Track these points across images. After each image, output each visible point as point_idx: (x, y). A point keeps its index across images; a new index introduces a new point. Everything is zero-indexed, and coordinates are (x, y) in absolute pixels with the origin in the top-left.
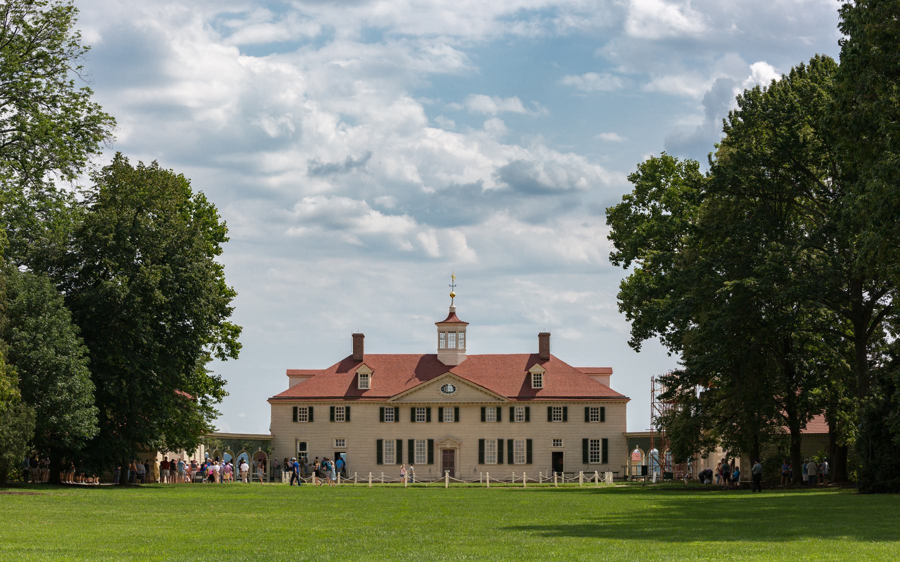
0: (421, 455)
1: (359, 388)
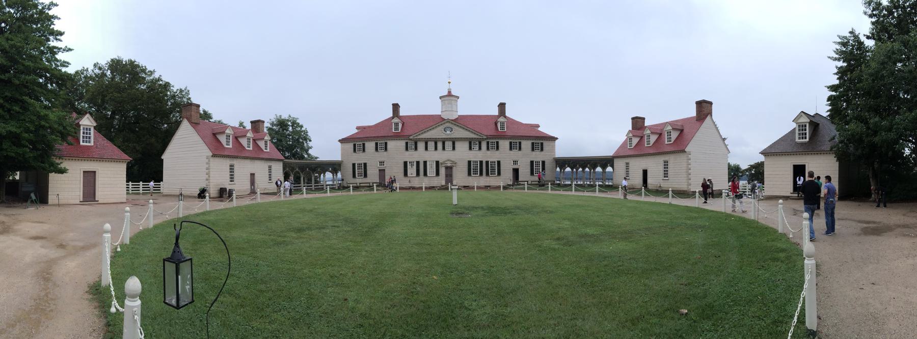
0: (431, 171)
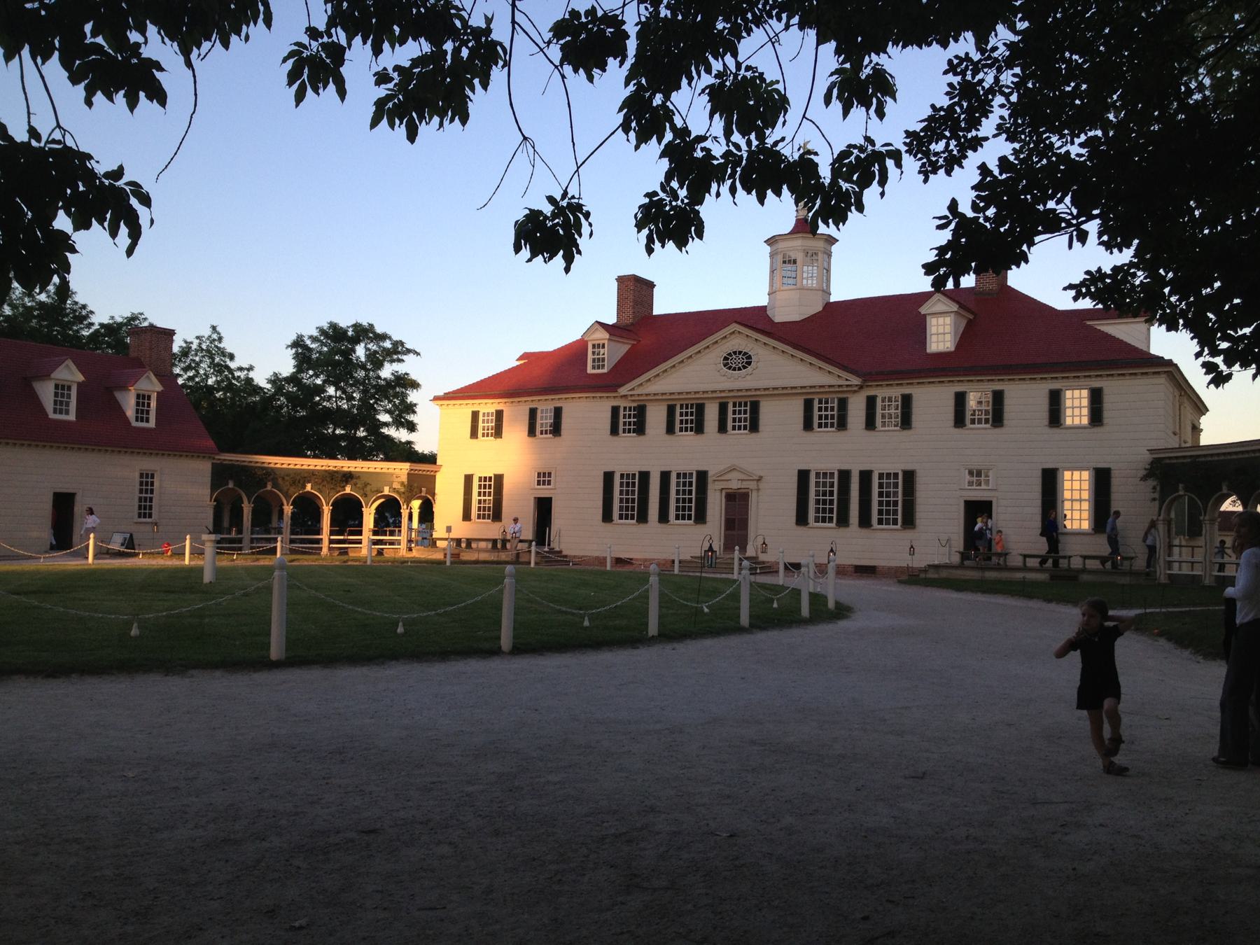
1: (590, 370)
